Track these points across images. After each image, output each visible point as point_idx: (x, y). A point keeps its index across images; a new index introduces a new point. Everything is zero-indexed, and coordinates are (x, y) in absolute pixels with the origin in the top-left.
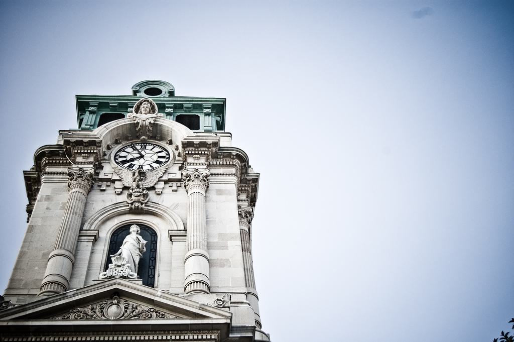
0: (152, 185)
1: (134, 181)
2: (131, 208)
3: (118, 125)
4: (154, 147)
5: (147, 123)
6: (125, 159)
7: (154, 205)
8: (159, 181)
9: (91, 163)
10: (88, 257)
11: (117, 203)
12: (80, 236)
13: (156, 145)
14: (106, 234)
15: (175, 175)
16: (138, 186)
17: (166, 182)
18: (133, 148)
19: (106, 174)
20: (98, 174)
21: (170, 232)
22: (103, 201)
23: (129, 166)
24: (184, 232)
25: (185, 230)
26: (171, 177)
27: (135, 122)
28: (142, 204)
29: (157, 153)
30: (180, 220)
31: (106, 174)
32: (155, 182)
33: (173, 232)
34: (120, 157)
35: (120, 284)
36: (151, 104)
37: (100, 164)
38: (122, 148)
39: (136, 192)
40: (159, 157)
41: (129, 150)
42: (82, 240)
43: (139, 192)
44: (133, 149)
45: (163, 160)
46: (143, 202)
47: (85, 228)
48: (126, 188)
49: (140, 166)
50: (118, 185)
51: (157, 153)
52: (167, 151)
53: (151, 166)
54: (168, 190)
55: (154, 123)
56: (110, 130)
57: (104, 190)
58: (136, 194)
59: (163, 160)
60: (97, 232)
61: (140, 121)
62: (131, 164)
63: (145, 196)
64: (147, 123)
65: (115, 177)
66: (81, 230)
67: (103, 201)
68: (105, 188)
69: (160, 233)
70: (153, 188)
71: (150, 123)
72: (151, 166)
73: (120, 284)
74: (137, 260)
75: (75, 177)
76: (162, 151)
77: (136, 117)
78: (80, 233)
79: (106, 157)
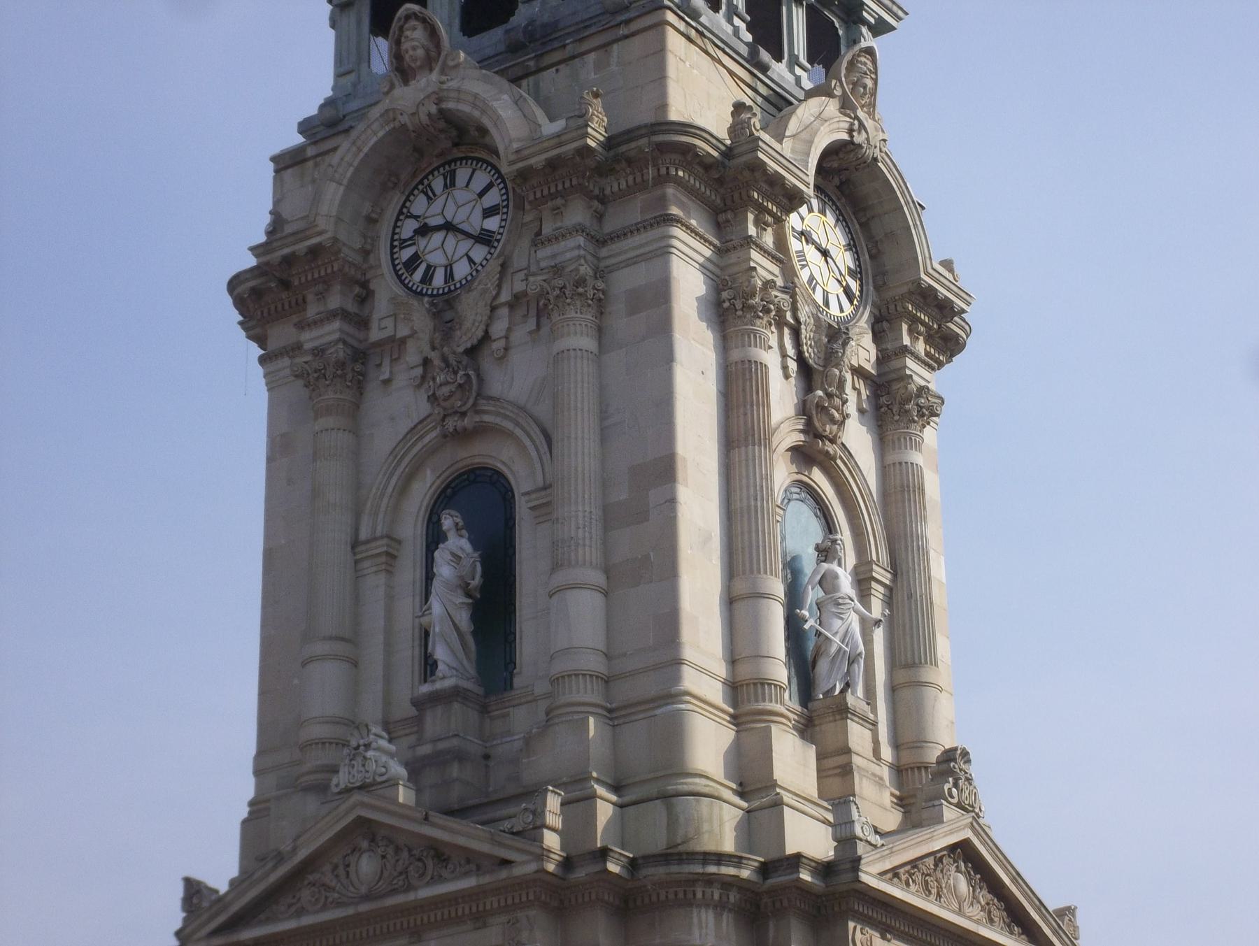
0: (480, 334)
2: (445, 436)
3: (362, 155)
5: (424, 119)
9: (332, 315)
11: (416, 426)
13: (478, 160)
14: (411, 529)
16: (444, 359)
17: (512, 306)
18: (426, 194)
22: (392, 419)
27: (397, 124)
28: (463, 414)
29: (481, 194)
33: (533, 496)
34: (404, 244)
35: (363, 805)
38: (404, 206)
39: (441, 385)
41: (419, 205)
42: (366, 572)
43: (447, 383)
44: (429, 198)
45: (492, 224)
46: (464, 409)
47: (363, 535)
49: (446, 267)
50: (412, 356)
51: (481, 194)
53: (471, 260)
55: (441, 111)
56: (345, 182)
57: (387, 382)
58: (445, 390)
59: (492, 224)
61: (405, 119)
64: (424, 119)
65: (403, 332)
66: (355, 544)
67: (392, 419)
70: (486, 337)
71: (429, 115)
72: (471, 260)
73: (363, 805)
74: (463, 618)
76: (489, 187)
77: (394, 110)
78: (355, 554)
79: (372, 258)
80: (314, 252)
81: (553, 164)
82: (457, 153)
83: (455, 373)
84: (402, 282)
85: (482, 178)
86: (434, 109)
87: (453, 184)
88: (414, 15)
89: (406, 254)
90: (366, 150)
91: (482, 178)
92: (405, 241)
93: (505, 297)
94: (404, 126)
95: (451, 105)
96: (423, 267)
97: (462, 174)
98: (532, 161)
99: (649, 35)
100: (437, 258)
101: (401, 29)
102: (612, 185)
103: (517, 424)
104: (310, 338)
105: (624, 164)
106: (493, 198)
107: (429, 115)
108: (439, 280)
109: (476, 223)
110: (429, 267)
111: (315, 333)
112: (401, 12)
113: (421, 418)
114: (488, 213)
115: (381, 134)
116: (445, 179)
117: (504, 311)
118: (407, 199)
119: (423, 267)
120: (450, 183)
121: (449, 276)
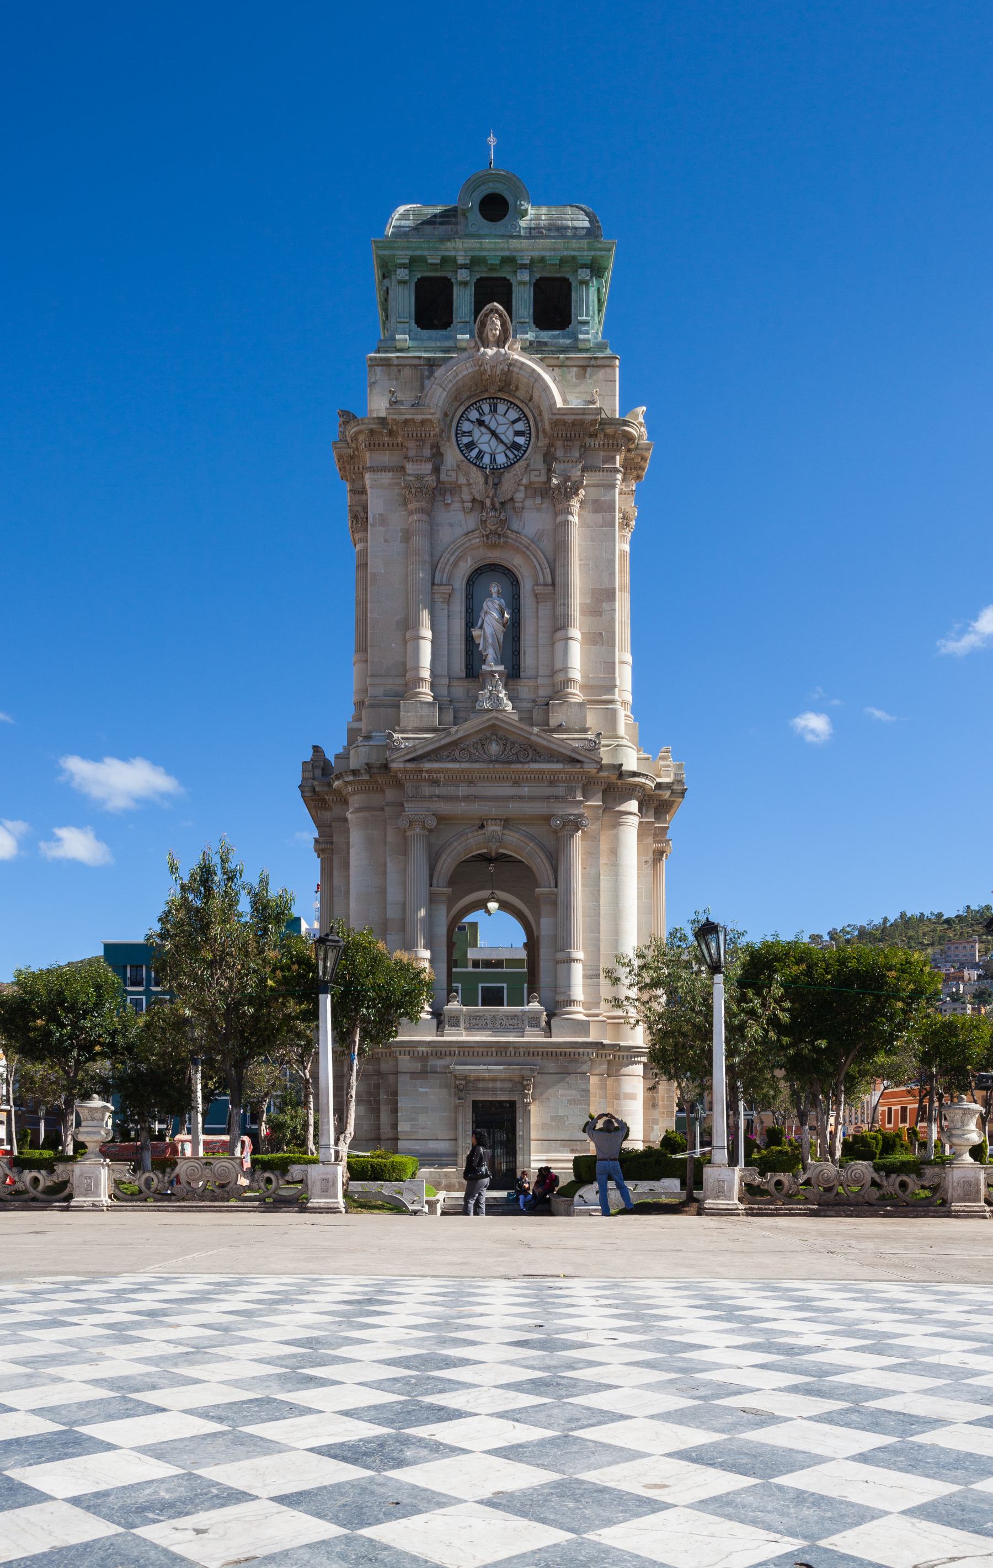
0: (509, 497)
1: (488, 497)
4: (509, 408)
6: (471, 439)
7: (513, 536)
8: (518, 485)
10: (445, 628)
11: (469, 533)
12: (433, 593)
13: (512, 403)
14: (459, 584)
15: (537, 473)
16: (493, 504)
18: (478, 411)
19: (450, 473)
20: (437, 470)
21: (536, 588)
23: (477, 457)
24: (552, 588)
25: (553, 584)
26: (534, 479)
29: (514, 422)
30: (547, 566)
31: (450, 473)
32: (513, 490)
36: (501, 316)
37: (438, 447)
38: (464, 413)
40: (518, 433)
48: (474, 500)
51: (514, 422)
52: (527, 419)
54: (528, 503)
55: (509, 369)
56: (447, 390)
59: (521, 440)
60: (451, 587)
62: (480, 451)
63: (503, 523)
64: (498, 372)
65: (462, 480)
66: (433, 584)
68: (449, 502)
69: (524, 582)
70: (512, 499)
71: (502, 370)
75: (413, 490)
80: (423, 422)
81: (574, 424)
82: (500, 395)
83: (500, 513)
84: (464, 455)
85: (513, 415)
86: (506, 369)
87: (495, 411)
88: (497, 311)
89: (466, 440)
90: (460, 376)
91: (513, 415)
92: (465, 432)
93: (524, 481)
94: (485, 371)
95: (516, 369)
96: (476, 451)
97: (501, 408)
98: (566, 417)
99: (608, 370)
100: (485, 448)
101: (486, 315)
102: (590, 442)
103: (528, 548)
104: (410, 468)
105: (603, 435)
106: (520, 426)
107: (502, 370)
108: (486, 460)
109: (509, 437)
110: (480, 451)
111: (415, 467)
112: (488, 306)
113: (470, 530)
114: (518, 433)
115: (470, 370)
116: (491, 407)
117: (522, 488)
118: (466, 410)
119: (476, 451)
120: (494, 410)
121: (493, 459)
